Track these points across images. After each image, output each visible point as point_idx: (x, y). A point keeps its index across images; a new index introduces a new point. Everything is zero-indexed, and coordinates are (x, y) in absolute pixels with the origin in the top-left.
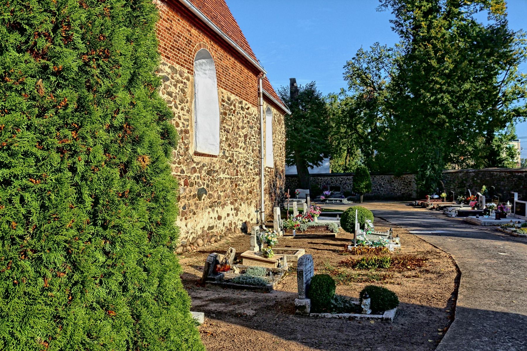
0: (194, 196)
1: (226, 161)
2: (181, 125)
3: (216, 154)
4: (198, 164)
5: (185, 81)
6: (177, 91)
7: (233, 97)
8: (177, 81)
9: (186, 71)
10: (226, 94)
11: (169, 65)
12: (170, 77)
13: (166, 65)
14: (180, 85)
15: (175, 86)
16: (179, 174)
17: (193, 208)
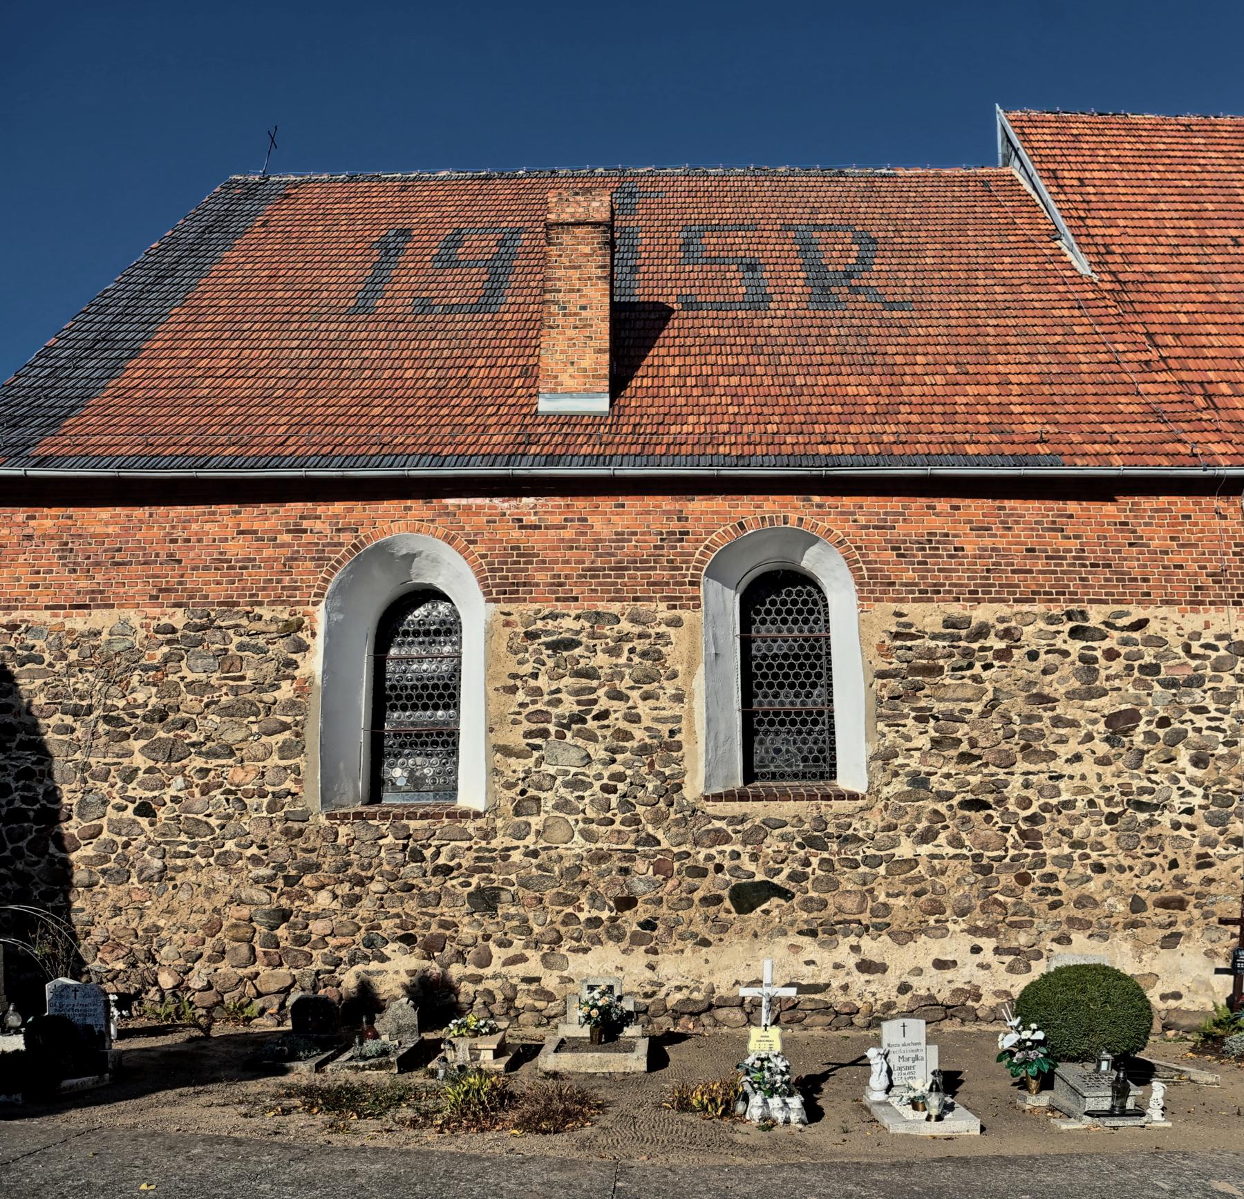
0: (712, 900)
1: (942, 807)
2: (639, 733)
3: (861, 789)
4: (733, 820)
5: (663, 629)
6: (622, 660)
7: (982, 613)
8: (623, 638)
9: (663, 606)
10: (927, 617)
11: (573, 613)
12: (583, 638)
13: (563, 616)
14: (641, 645)
15: (613, 652)
16: (628, 846)
17: (702, 930)
